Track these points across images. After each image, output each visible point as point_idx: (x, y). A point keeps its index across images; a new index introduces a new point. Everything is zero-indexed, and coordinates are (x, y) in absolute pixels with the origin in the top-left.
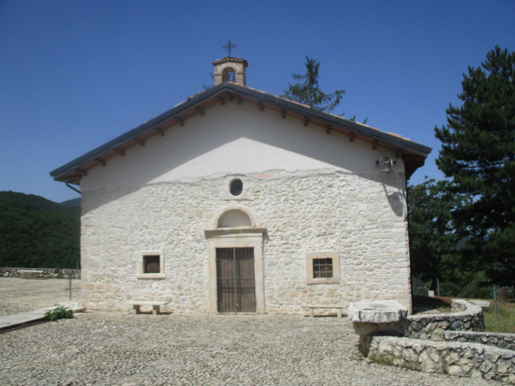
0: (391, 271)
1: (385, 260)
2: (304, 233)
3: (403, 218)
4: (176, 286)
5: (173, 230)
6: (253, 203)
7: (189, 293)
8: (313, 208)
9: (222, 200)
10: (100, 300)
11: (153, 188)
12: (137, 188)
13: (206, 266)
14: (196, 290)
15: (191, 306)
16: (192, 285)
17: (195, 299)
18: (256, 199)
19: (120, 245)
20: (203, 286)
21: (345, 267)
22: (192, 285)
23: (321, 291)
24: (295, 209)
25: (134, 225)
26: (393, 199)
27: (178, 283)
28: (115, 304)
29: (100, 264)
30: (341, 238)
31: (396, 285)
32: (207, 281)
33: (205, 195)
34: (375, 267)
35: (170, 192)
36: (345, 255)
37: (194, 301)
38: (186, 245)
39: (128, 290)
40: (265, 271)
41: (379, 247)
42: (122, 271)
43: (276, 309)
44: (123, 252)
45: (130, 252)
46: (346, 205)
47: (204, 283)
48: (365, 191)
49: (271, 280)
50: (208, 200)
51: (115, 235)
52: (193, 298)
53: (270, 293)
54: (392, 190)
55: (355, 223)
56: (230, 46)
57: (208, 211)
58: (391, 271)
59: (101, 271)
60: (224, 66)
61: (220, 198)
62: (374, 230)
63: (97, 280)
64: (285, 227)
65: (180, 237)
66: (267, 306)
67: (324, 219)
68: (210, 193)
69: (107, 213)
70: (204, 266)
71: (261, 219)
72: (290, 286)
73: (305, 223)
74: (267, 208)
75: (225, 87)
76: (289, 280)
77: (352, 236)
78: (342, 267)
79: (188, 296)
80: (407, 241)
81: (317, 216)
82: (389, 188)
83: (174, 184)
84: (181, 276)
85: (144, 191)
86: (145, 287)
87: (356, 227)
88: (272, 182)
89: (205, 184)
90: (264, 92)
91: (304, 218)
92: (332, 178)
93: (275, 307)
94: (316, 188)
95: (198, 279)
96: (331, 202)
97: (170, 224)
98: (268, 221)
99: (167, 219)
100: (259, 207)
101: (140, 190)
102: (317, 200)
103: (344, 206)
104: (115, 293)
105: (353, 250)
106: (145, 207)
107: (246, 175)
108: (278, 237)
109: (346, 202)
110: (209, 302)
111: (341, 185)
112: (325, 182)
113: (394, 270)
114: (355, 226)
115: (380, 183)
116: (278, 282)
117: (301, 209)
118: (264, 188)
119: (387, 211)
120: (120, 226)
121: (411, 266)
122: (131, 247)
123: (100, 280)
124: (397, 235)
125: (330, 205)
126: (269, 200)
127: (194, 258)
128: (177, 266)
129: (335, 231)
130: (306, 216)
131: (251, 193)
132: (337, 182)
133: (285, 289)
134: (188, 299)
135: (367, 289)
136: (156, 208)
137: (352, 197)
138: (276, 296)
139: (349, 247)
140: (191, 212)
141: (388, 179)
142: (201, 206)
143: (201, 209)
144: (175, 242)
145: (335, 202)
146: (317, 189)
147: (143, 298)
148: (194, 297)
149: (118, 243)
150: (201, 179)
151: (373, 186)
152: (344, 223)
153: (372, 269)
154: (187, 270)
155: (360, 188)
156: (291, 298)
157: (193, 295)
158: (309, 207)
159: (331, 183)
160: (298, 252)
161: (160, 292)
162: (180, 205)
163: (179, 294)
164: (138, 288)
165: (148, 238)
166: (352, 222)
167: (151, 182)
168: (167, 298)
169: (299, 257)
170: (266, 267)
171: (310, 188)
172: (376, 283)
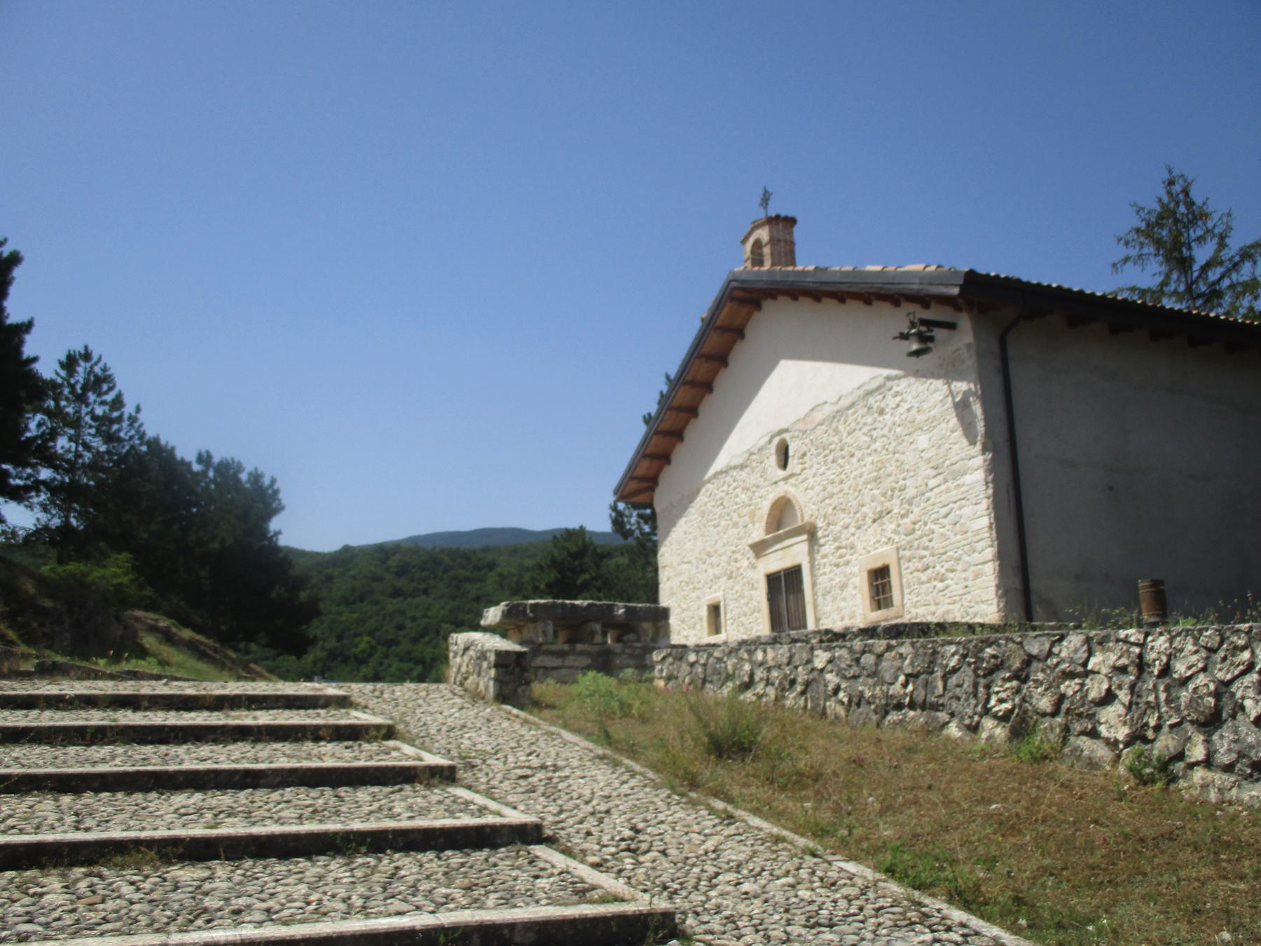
3: (979, 447)
6: (801, 478)
11: (709, 486)
26: (962, 407)
34: (947, 570)
54: (961, 386)
150: (746, 455)
153: (943, 575)
167: (706, 477)
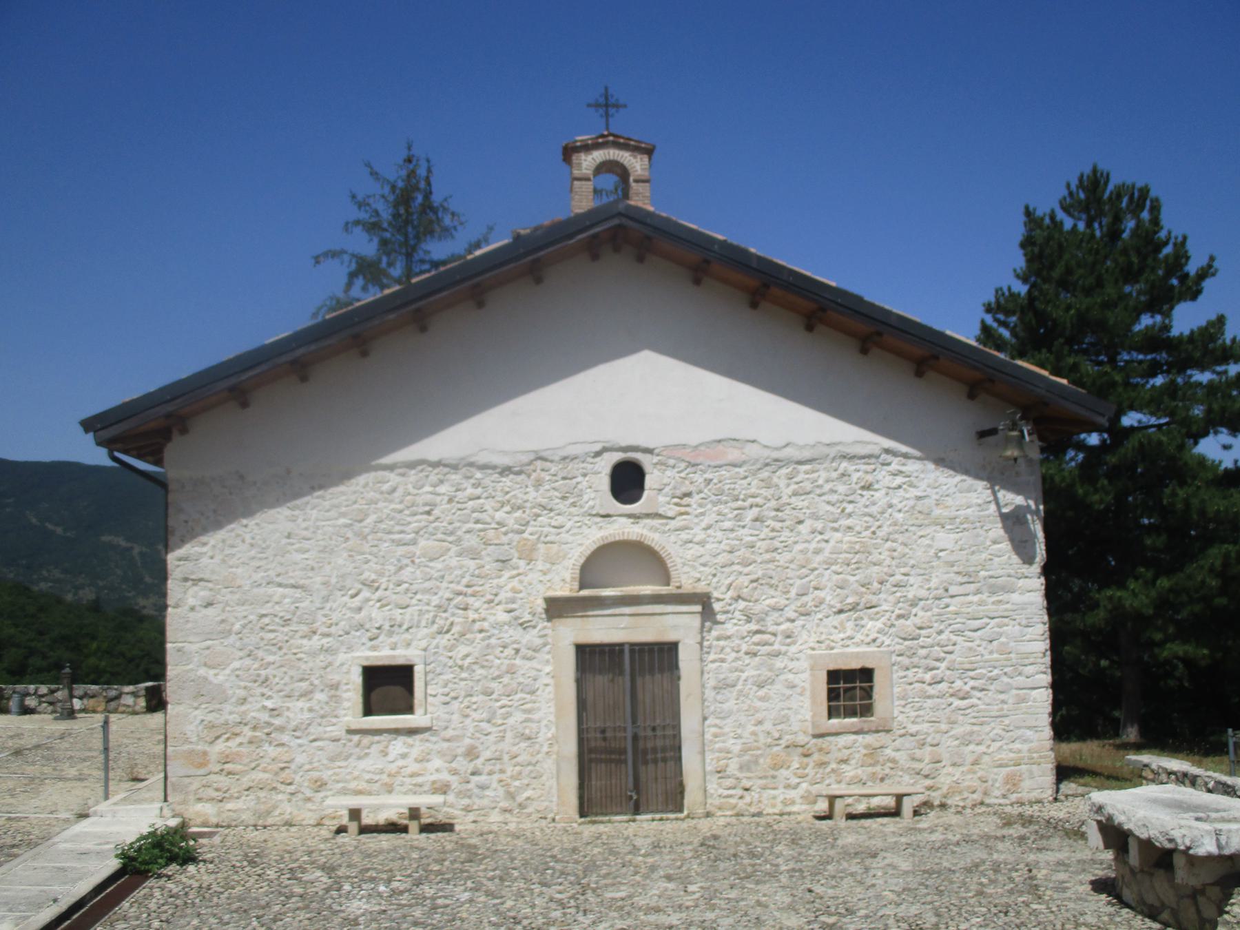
0: (1010, 697)
1: (996, 672)
2: (804, 605)
3: (1036, 568)
4: (460, 751)
5: (451, 596)
6: (673, 524)
7: (498, 767)
8: (827, 541)
9: (590, 515)
10: (227, 795)
11: (393, 478)
12: (346, 476)
13: (546, 694)
14: (518, 759)
15: (504, 804)
16: (505, 746)
17: (517, 783)
18: (682, 514)
19: (291, 637)
20: (537, 746)
21: (905, 690)
22: (505, 746)
23: (847, 752)
24: (782, 542)
25: (334, 580)
26: (1013, 522)
27: (467, 741)
28: (275, 807)
29: (230, 692)
30: (894, 616)
31: (1020, 732)
32: (549, 735)
33: (544, 501)
34: (973, 688)
35: (442, 489)
36: (905, 661)
37: (512, 789)
38: (489, 637)
39: (316, 765)
40: (706, 704)
41: (982, 640)
42: (297, 711)
43: (733, 801)
44: (299, 656)
45: (322, 657)
46: (907, 534)
47: (540, 739)
48: (949, 501)
49: (720, 728)
50: (552, 514)
51: (277, 607)
52: (509, 780)
53: (719, 760)
54: (1012, 500)
55: (928, 580)
56: (607, 105)
57: (552, 543)
58: (1010, 697)
59: (231, 713)
60: (598, 156)
61: (586, 509)
62: (970, 598)
63: (217, 738)
64: (756, 588)
65: (472, 615)
66: (712, 795)
67: (854, 570)
68: (556, 494)
69: (252, 545)
70: (538, 693)
71: (694, 568)
72: (769, 740)
73: (807, 579)
74: (711, 539)
75: (620, 214)
76: (767, 726)
77: (921, 613)
78: (896, 690)
79: (496, 777)
80: (1045, 624)
81: (835, 563)
82: (1004, 496)
83: (455, 467)
84: (474, 720)
85: (366, 485)
86: (367, 754)
87: (929, 589)
88: (724, 472)
89: (543, 470)
90: (720, 237)
91: (804, 567)
92: (873, 467)
93: (730, 796)
94: (833, 491)
95: (525, 728)
96: (870, 527)
97: (443, 577)
98: (714, 572)
99: (431, 564)
100: (690, 537)
101: (353, 481)
102: (835, 521)
103: (901, 538)
104: (276, 774)
105: (923, 647)
106: (367, 530)
107: (656, 451)
108: (737, 614)
109: (906, 527)
110: (554, 791)
111: (894, 485)
112: (855, 476)
113: (1017, 695)
114: (927, 587)
115: (985, 483)
116: (739, 731)
117: (796, 543)
118: (702, 485)
119: (1000, 550)
120: (292, 581)
121: (1056, 686)
122: (325, 640)
123: (228, 739)
124: (1023, 609)
125: (868, 533)
126: (714, 517)
127: (511, 671)
128: (463, 693)
129: (879, 600)
130: (808, 561)
131: (668, 499)
132: (883, 477)
133: (758, 749)
134: (495, 785)
135: (957, 742)
136: (402, 532)
137: (919, 515)
138: (733, 767)
139: (913, 639)
140: (503, 545)
141: (1003, 474)
142: (530, 529)
143: (531, 537)
144: (455, 629)
145: (879, 527)
146: (836, 492)
147: (362, 785)
148: (514, 778)
149: (286, 629)
150: (532, 456)
151: (969, 491)
152: (901, 581)
153: (968, 692)
154: (491, 704)
155: (937, 493)
156: (772, 772)
157: (509, 773)
158: (817, 539)
159: (870, 478)
160: (789, 654)
161: (414, 767)
162: (470, 525)
163: (469, 771)
164: (346, 759)
165: (377, 615)
166: (920, 578)
168: (434, 782)
169: (791, 665)
170: (709, 694)
171: (818, 491)
172: (976, 728)
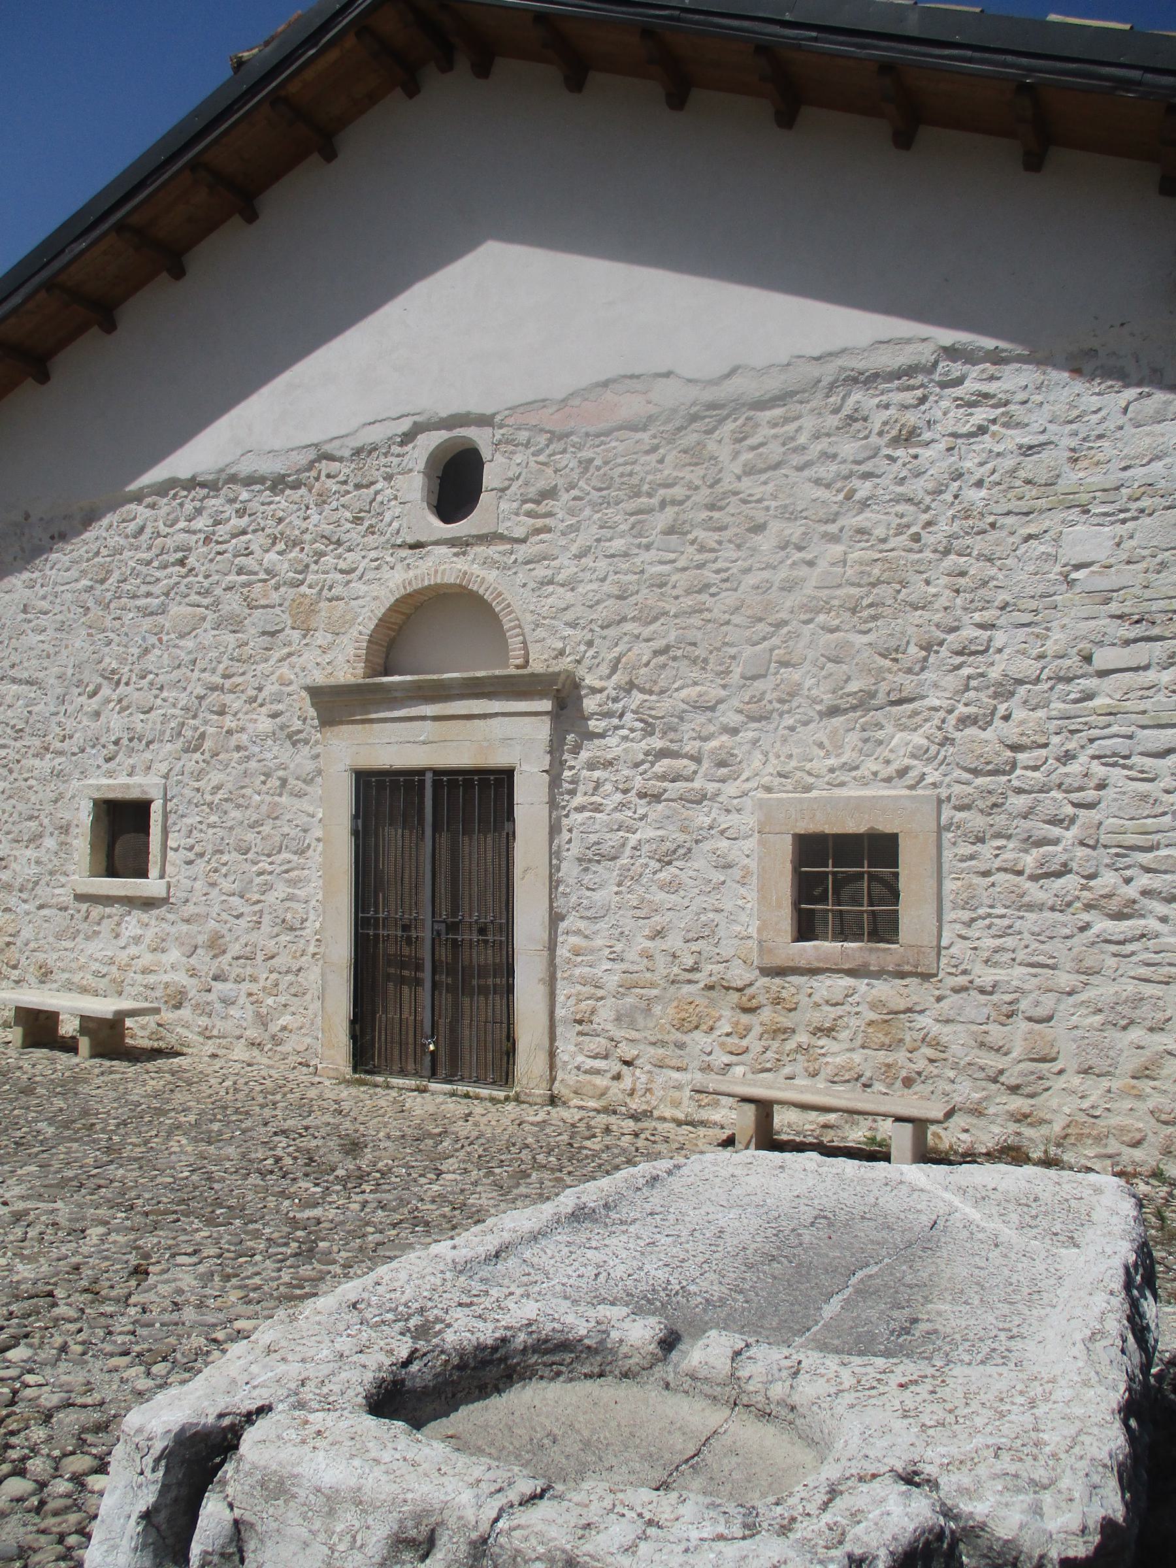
2: (758, 699)
4: (201, 939)
5: (203, 692)
6: (522, 551)
8: (811, 564)
9: (393, 546)
11: (140, 511)
15: (252, 1033)
18: (538, 531)
24: (718, 572)
30: (952, 719)
33: (327, 529)
34: (1145, 893)
35: (200, 523)
36: (975, 821)
37: (264, 1011)
43: (601, 1082)
44: (32, 782)
46: (993, 535)
51: (10, 713)
57: (338, 599)
62: (1151, 676)
64: (664, 666)
65: (229, 722)
71: (554, 631)
72: (676, 970)
73: (766, 644)
74: (587, 576)
76: (674, 942)
77: (1019, 714)
79: (246, 986)
83: (212, 486)
86: (97, 933)
87: (1041, 657)
89: (328, 476)
91: (760, 620)
93: (598, 1072)
96: (908, 526)
98: (589, 637)
99: (182, 643)
103: (979, 544)
105: (1019, 791)
108: (629, 716)
109: (991, 519)
116: (618, 947)
117: (748, 570)
120: (25, 675)
125: (903, 540)
128: (210, 849)
129: (921, 684)
131: (515, 505)
133: (653, 985)
134: (242, 1000)
136: (148, 595)
138: (605, 1015)
142: (311, 578)
144: (208, 744)
145: (929, 524)
147: (89, 980)
149: (18, 744)
150: (312, 454)
154: (246, 866)
159: (912, 418)
161: (147, 959)
162: (232, 578)
165: (116, 722)
167: (133, 487)
169: (725, 821)
170: (569, 870)
171: (796, 460)
172: (1148, 990)
